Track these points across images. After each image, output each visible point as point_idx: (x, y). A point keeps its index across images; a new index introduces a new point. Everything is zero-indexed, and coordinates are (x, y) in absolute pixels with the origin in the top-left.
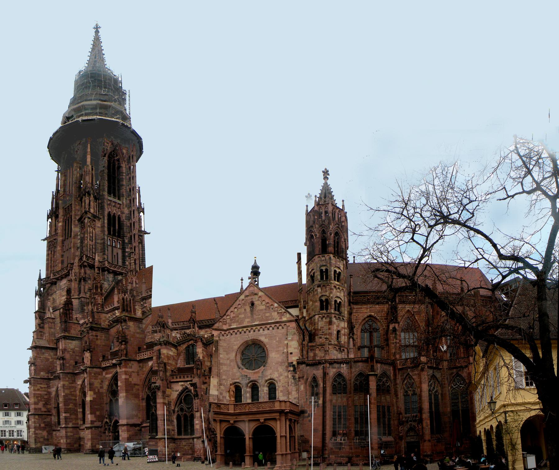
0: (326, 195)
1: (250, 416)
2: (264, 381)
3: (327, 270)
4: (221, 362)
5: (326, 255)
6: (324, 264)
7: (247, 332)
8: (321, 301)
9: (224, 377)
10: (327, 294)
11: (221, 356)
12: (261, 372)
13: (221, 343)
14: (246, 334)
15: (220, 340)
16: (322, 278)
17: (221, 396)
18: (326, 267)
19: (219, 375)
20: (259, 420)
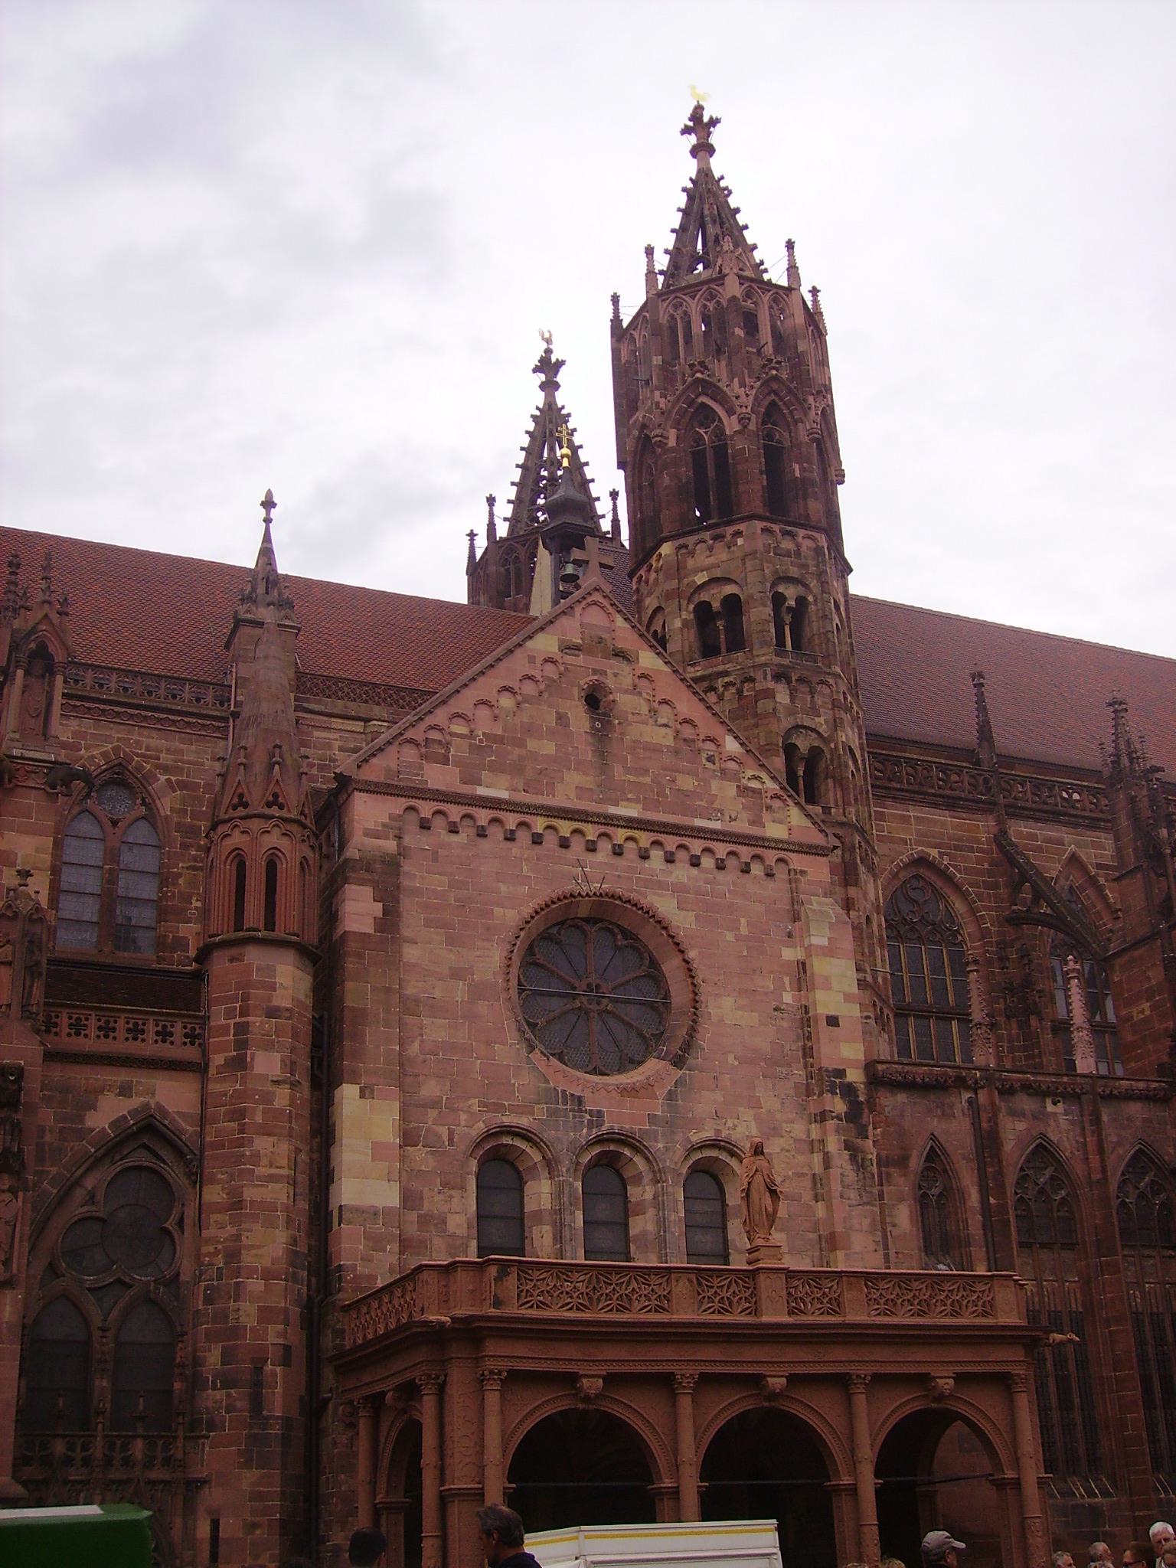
0: (708, 211)
1: (712, 1352)
2: (680, 1150)
3: (801, 601)
4: (410, 991)
5: (801, 532)
6: (794, 572)
7: (577, 845)
8: (790, 750)
9: (430, 1089)
10: (821, 722)
11: (411, 953)
12: (661, 1092)
13: (414, 875)
14: (570, 855)
15: (403, 852)
16: (780, 642)
17: (413, 1216)
18: (800, 590)
19: (403, 1076)
20: (756, 1381)
